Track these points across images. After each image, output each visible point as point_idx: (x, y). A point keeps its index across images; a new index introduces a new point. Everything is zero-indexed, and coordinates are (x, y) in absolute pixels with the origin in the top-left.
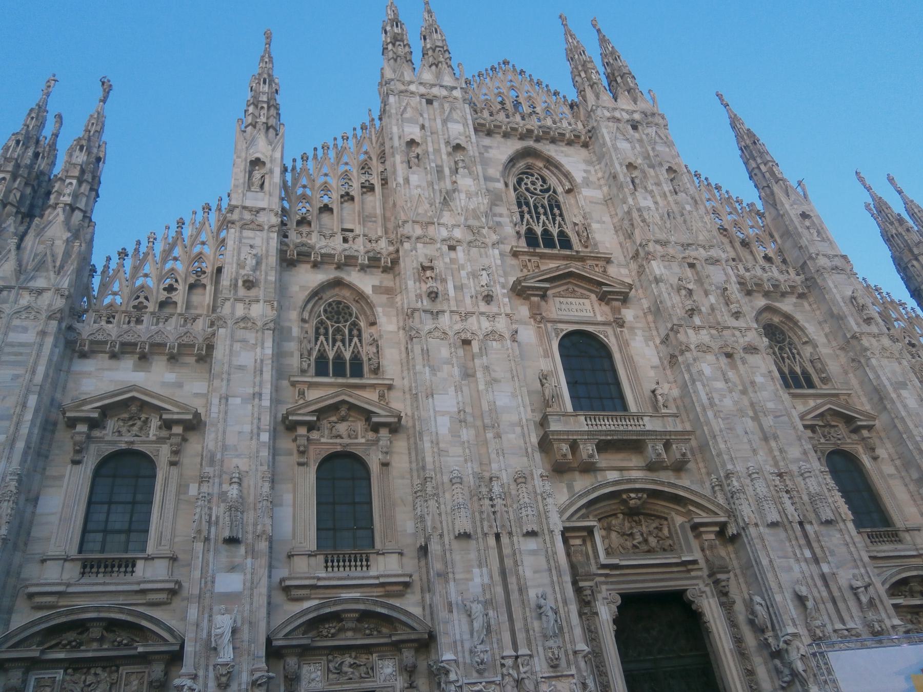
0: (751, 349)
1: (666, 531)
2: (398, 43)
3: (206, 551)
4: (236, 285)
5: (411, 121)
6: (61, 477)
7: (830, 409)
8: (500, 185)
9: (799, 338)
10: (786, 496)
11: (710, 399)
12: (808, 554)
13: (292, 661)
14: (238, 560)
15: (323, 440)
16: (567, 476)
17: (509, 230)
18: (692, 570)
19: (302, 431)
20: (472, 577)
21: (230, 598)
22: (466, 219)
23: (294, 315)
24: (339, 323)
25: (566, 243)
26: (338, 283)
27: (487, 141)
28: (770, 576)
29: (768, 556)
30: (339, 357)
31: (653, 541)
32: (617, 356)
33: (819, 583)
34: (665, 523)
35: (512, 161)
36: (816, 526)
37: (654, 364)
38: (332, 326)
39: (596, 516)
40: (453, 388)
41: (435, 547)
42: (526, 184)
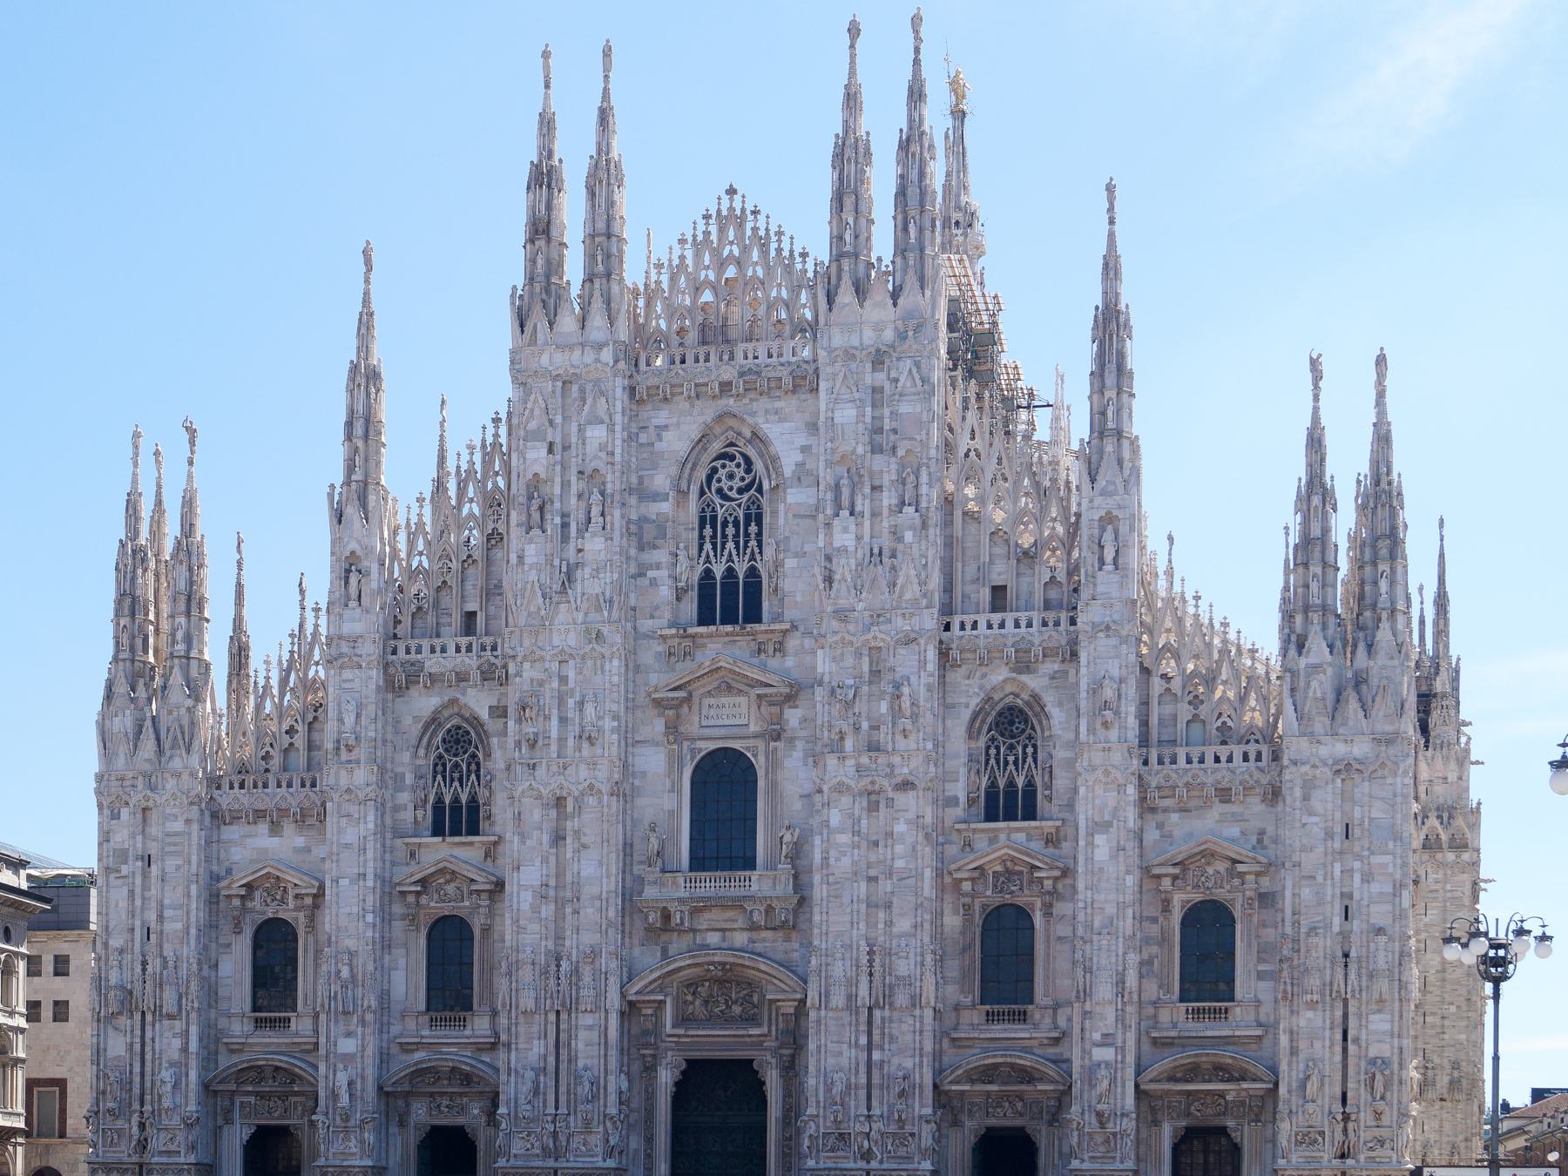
0: (906, 785)
1: (755, 999)
3: (328, 1021)
4: (338, 749)
6: (229, 945)
10: (864, 979)
12: (863, 1040)
13: (400, 1103)
14: (352, 1028)
15: (432, 904)
16: (665, 937)
17: (665, 592)
19: (411, 899)
20: (531, 1048)
21: (347, 1058)
23: (406, 757)
24: (456, 755)
27: (662, 416)
28: (812, 1062)
30: (456, 800)
32: (761, 783)
33: (863, 1069)
35: (703, 440)
36: (887, 1013)
41: (503, 1021)
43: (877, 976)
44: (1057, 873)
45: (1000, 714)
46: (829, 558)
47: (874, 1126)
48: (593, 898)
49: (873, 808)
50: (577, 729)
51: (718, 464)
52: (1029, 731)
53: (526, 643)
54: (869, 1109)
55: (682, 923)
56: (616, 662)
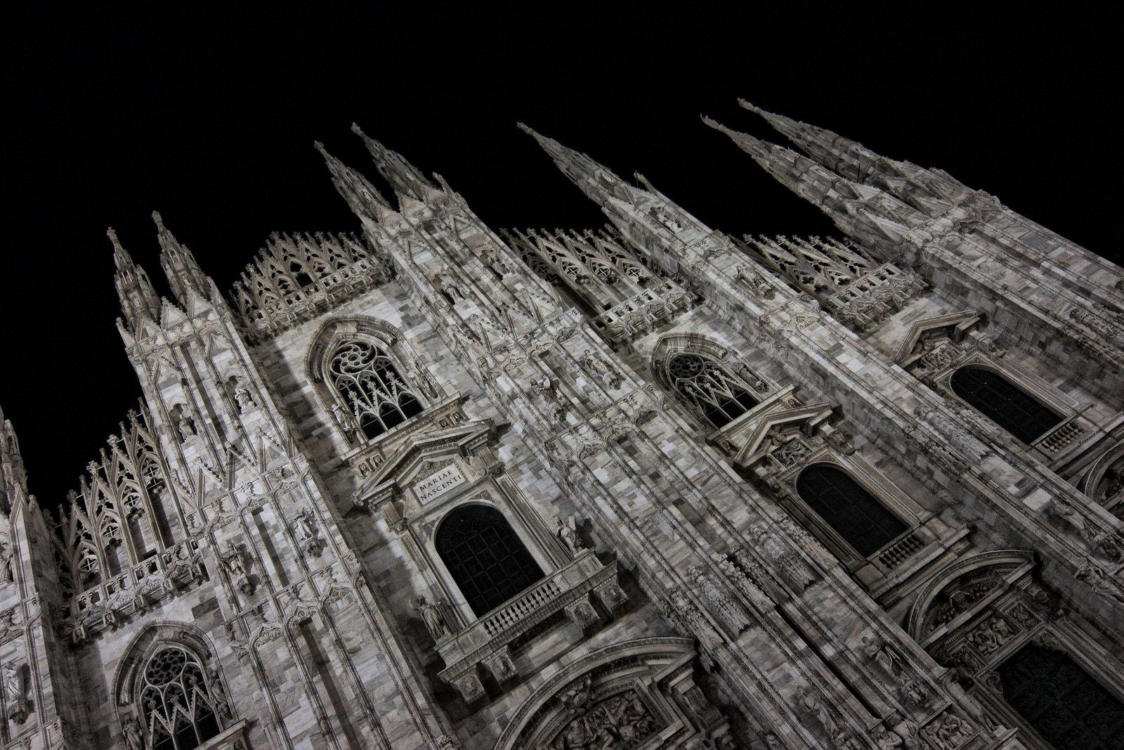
0: (646, 417)
1: (639, 708)
2: (131, 296)
5: (170, 382)
7: (773, 427)
8: (309, 389)
9: (715, 355)
10: (746, 583)
11: (619, 510)
12: (801, 644)
17: (337, 436)
18: (685, 743)
22: (264, 466)
25: (412, 407)
26: (151, 629)
29: (753, 677)
30: (182, 724)
31: (627, 732)
32: (508, 514)
33: (828, 675)
34: (634, 696)
36: (798, 601)
37: (555, 497)
38: (162, 690)
39: (545, 742)
40: (304, 695)
42: (345, 364)
43: (757, 572)
44: (828, 413)
45: (672, 367)
46: (464, 325)
47: (902, 728)
48: (389, 698)
49: (631, 451)
50: (295, 552)
51: (339, 357)
52: (704, 363)
53: (211, 515)
54: (874, 712)
55: (508, 669)
56: (311, 483)
